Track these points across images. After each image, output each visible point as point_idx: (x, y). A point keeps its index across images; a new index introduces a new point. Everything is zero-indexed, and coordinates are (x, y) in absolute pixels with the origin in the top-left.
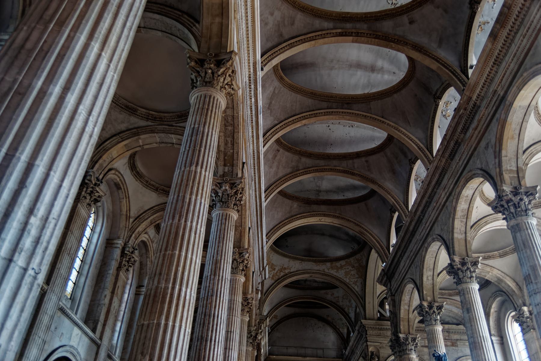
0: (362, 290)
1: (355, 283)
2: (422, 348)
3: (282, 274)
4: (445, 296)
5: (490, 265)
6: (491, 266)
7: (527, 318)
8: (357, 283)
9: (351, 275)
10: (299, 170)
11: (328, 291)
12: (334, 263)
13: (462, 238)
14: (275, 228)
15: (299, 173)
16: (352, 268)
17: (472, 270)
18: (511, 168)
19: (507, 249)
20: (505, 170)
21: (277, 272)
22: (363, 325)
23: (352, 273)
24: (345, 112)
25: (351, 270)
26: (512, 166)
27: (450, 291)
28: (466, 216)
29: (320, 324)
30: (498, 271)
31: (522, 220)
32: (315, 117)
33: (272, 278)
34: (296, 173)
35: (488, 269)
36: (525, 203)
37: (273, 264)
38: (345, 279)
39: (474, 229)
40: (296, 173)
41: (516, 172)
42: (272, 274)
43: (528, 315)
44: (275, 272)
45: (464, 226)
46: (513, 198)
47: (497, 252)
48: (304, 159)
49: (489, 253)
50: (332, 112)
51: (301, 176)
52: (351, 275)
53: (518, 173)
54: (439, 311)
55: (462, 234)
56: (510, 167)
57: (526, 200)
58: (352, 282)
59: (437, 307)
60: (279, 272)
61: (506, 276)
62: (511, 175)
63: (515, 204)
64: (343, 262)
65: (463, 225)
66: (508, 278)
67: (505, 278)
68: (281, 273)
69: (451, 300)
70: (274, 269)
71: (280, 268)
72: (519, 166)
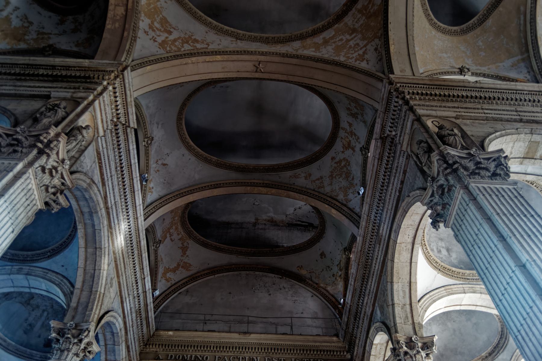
0: (380, 60)
1: (361, 58)
3: (187, 47)
8: (366, 56)
9: (350, 47)
11: (298, 171)
12: (308, 40)
16: (351, 35)
21: (175, 40)
22: (397, 90)
23: (352, 43)
25: (347, 41)
29: (284, 283)
37: (167, 22)
38: (336, 58)
42: (163, 38)
44: (171, 37)
52: (350, 47)
58: (352, 58)
64: (328, 34)
68: (185, 45)
70: (170, 33)
71: (183, 36)
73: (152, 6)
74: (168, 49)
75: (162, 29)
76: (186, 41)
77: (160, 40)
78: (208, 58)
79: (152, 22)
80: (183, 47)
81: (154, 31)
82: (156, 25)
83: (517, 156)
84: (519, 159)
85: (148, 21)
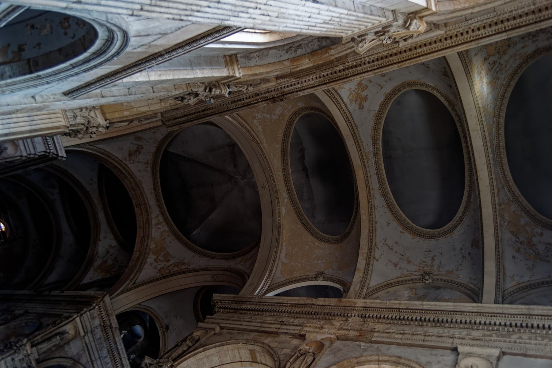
3: (176, 269)
33: (160, 270)
37: (168, 253)
42: (161, 266)
44: (168, 264)
60: (173, 266)
70: (168, 261)
73: (160, 247)
74: (163, 272)
75: (164, 260)
76: (176, 265)
77: (159, 267)
78: (184, 275)
79: (158, 257)
80: (173, 269)
81: (157, 262)
82: (160, 258)
83: (247, 360)
84: (249, 363)
85: (154, 257)
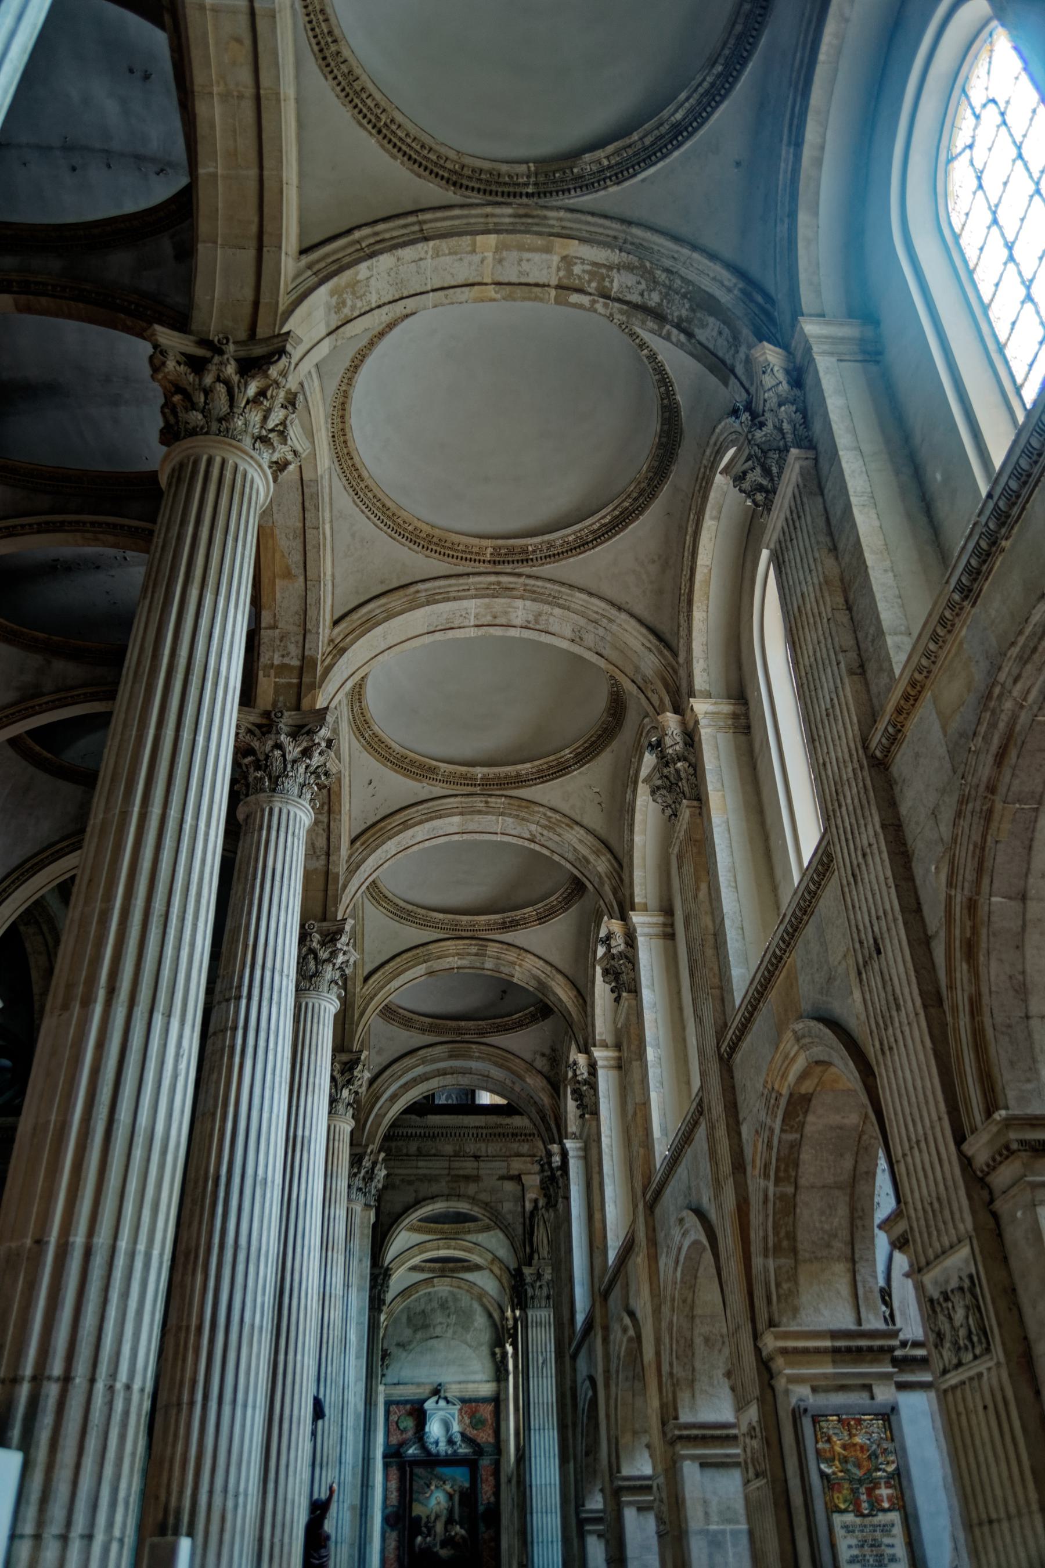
2: (500, 1182)
4: (467, 1037)
5: (518, 943)
6: (521, 948)
7: (586, 1082)
10: (43, 695)
13: (316, 869)
14: (28, 865)
15: (40, 705)
17: (324, 955)
18: (286, 661)
19: (552, 898)
20: (265, 666)
24: (100, 524)
26: (288, 654)
27: (480, 1022)
28: (326, 807)
30: (537, 960)
31: (257, 803)
32: (10, 535)
34: (30, 704)
35: (511, 956)
36: (284, 756)
39: (362, 845)
40: (30, 704)
41: (296, 672)
43: (586, 1076)
45: (325, 835)
46: (256, 744)
47: (531, 909)
48: (59, 665)
49: (514, 913)
50: (62, 523)
51: (45, 711)
53: (300, 677)
54: (347, 1076)
55: (318, 857)
56: (283, 656)
57: (291, 748)
59: (345, 1064)
61: (554, 972)
62: (283, 681)
63: (258, 760)
65: (321, 832)
66: (559, 978)
67: (553, 980)
69: (482, 1047)
72: (306, 653)
